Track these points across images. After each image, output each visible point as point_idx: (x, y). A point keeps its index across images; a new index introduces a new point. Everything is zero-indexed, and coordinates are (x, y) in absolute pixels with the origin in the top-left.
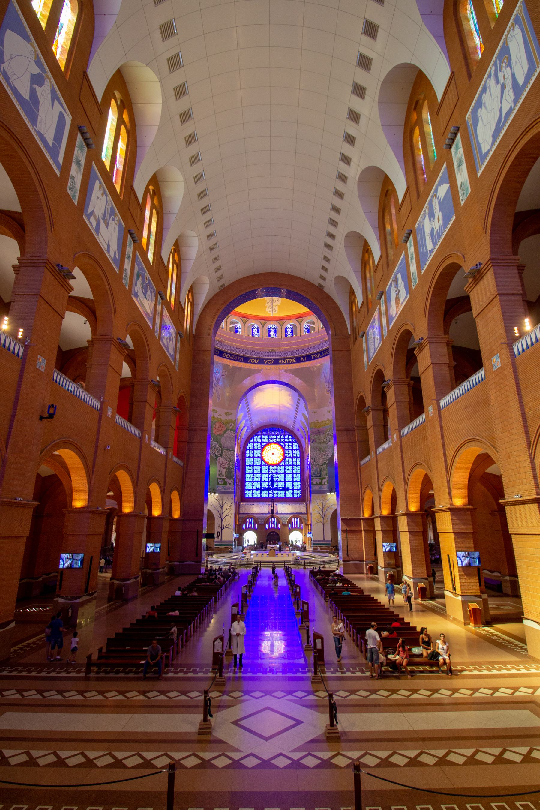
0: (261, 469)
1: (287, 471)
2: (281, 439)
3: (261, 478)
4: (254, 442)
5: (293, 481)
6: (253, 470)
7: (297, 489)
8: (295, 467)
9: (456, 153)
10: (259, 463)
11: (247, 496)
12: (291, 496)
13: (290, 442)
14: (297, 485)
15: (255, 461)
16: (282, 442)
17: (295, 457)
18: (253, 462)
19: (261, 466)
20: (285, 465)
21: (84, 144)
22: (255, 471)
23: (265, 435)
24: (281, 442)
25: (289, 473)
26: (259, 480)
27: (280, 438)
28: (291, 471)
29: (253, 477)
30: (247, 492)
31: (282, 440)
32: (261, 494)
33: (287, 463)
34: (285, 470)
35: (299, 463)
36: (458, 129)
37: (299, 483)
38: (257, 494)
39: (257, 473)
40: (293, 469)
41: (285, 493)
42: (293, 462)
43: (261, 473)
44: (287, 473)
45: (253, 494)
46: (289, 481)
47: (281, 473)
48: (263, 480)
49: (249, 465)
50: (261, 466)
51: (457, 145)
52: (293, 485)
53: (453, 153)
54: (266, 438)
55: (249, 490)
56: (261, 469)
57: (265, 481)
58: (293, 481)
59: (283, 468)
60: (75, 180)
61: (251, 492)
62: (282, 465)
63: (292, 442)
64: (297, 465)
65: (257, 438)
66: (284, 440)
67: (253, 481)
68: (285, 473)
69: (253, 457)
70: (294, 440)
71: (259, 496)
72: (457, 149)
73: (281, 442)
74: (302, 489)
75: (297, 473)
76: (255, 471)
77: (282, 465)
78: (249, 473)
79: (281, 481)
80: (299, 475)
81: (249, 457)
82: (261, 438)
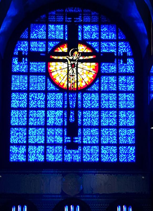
0: (46, 100)
1: (105, 105)
2: (91, 34)
3: (46, 118)
5: (118, 127)
6: (28, 101)
7: (127, 145)
8: (123, 96)
10: (41, 87)
11: (13, 158)
12: (114, 159)
13: (111, 41)
15: (31, 80)
16: (95, 40)
17: (123, 74)
18: (28, 83)
19: (46, 92)
20: (100, 92)
22: (32, 104)
23: (55, 24)
24: (92, 40)
25: (109, 109)
26: (42, 123)
28: (113, 105)
29: (28, 118)
30: (14, 149)
31: (94, 36)
32: (45, 153)
33: (104, 87)
34: (100, 101)
35: (131, 87)
37: (132, 131)
39: (37, 109)
40: (118, 101)
41: (100, 153)
42: (117, 83)
43: (46, 109)
44: (105, 109)
45: (27, 153)
46: (109, 127)
47: (91, 109)
48: (50, 122)
49: (20, 91)
50: (46, 92)
52: (118, 136)
55: (18, 145)
56: (46, 100)
57: (54, 127)
58: (118, 127)
59: (95, 97)
61: (23, 149)
62: (95, 92)
63: (117, 41)
64: (127, 92)
66: (100, 35)
67: (27, 127)
68: (100, 109)
69: (29, 73)
71: (41, 158)
73: (92, 40)
75: (126, 110)
76: (32, 104)
77: (95, 92)
78: (19, 109)
79: (91, 127)
80: (132, 115)
81: (19, 73)
82: (47, 31)
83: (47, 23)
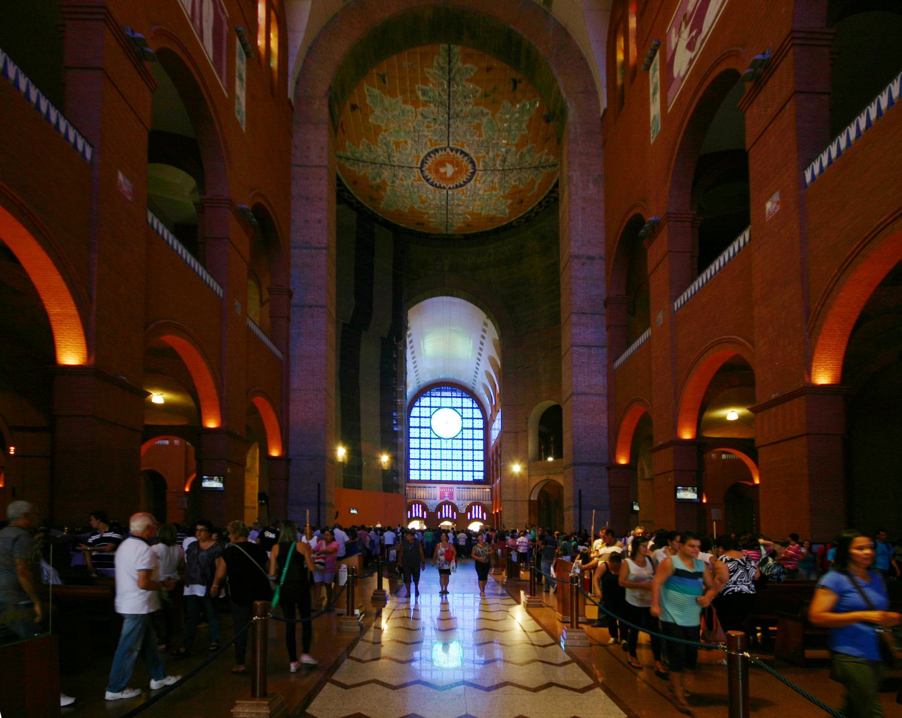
4: (420, 407)
9: (654, 74)
14: (480, 466)
21: (243, 51)
27: (457, 402)
36: (658, 46)
38: (425, 476)
51: (655, 66)
53: (651, 76)
54: (436, 402)
60: (241, 99)
63: (473, 408)
65: (425, 401)
70: (475, 405)
72: (655, 70)
74: (486, 471)
83: (431, 396)
